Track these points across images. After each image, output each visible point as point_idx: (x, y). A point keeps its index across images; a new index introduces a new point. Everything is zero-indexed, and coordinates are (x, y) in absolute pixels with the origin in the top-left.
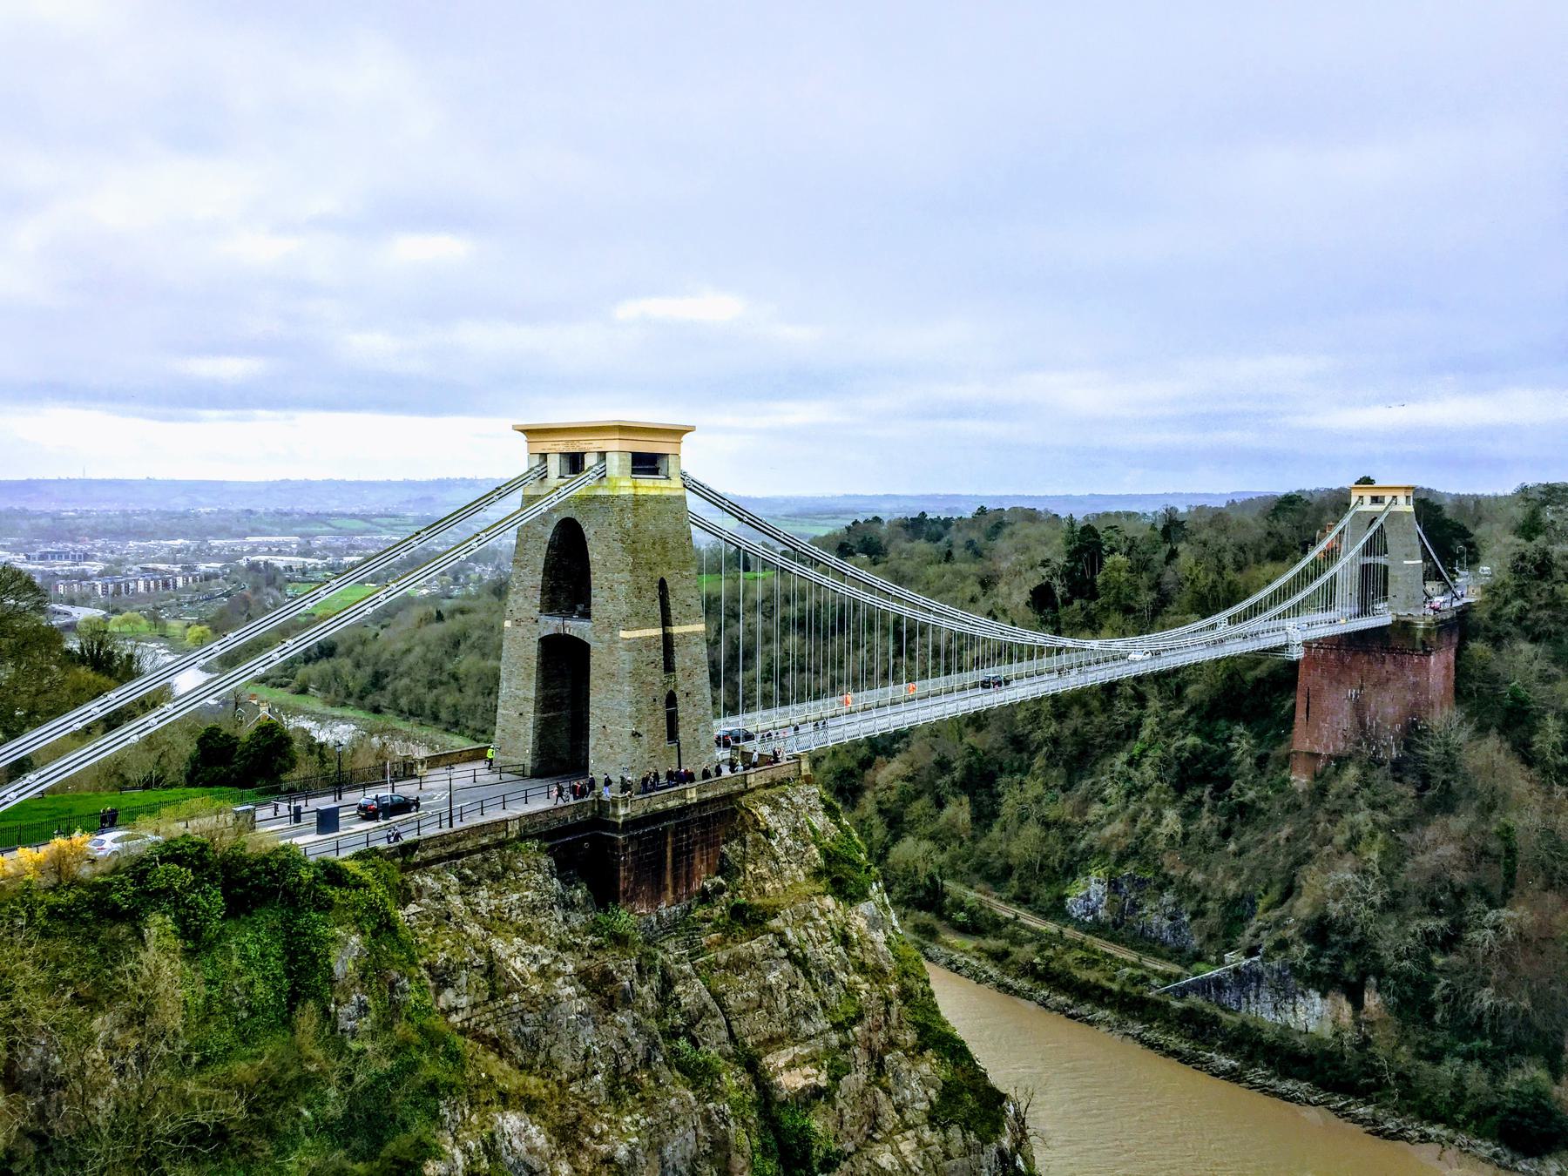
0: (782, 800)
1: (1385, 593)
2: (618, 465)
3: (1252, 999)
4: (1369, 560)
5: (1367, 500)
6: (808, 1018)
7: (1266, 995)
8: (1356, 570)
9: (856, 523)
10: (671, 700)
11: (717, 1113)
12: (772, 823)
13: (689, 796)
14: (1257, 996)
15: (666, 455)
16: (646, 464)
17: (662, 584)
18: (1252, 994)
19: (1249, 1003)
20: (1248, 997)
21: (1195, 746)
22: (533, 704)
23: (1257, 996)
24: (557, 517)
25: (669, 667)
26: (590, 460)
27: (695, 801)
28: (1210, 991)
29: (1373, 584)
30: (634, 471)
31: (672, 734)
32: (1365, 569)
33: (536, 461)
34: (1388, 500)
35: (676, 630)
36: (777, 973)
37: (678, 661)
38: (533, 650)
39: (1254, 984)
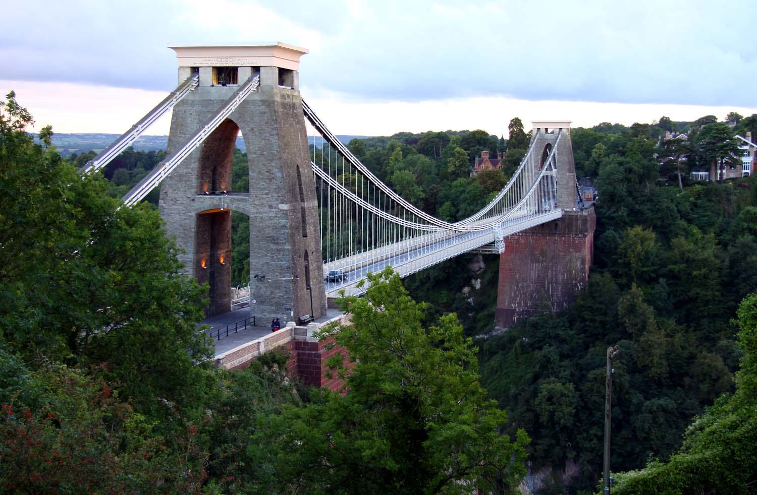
2: (270, 78)
15: (291, 71)
16: (284, 75)
29: (545, 191)
33: (189, 71)
35: (306, 205)
38: (192, 223)
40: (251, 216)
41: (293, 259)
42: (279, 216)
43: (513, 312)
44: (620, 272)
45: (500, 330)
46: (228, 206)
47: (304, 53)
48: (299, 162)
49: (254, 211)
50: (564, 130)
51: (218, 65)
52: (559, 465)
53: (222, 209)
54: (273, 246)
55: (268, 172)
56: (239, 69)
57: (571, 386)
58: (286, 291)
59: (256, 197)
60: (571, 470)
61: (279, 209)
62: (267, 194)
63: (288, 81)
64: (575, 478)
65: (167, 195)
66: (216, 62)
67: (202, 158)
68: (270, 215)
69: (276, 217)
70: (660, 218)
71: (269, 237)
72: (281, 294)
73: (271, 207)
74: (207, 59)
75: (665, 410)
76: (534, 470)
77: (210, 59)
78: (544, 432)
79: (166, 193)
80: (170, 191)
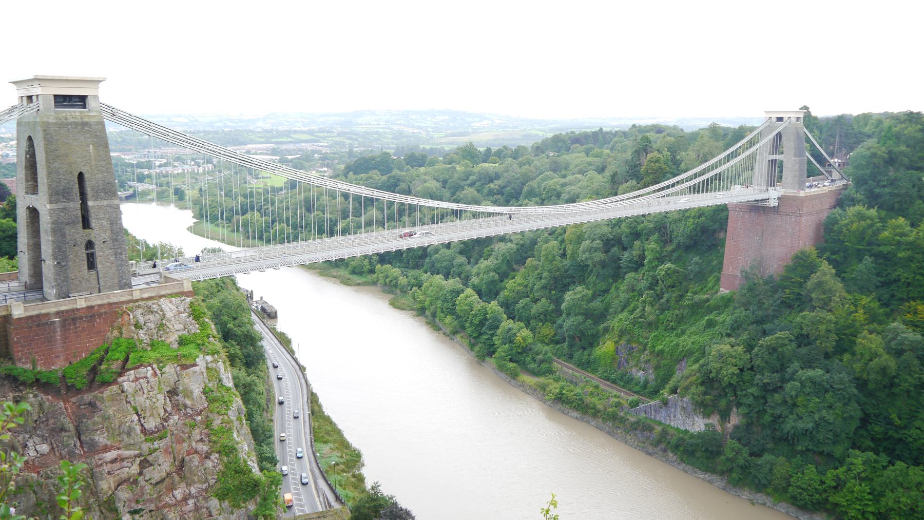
0: (154, 306)
1: (780, 178)
3: (672, 418)
4: (774, 157)
5: (774, 120)
6: (129, 434)
7: (679, 416)
8: (765, 164)
9: (567, 133)
10: (90, 245)
11: (54, 486)
12: (141, 320)
13: (78, 303)
14: (674, 416)
15: (86, 97)
17: (81, 176)
18: (672, 415)
19: (670, 420)
20: (670, 417)
21: (669, 269)
22: (26, 246)
23: (674, 416)
24: (27, 136)
25: (86, 224)
26: (34, 98)
27: (85, 306)
28: (651, 413)
29: (776, 172)
30: (56, 106)
31: (92, 265)
32: (773, 162)
33: (20, 99)
34: (785, 119)
35: (90, 203)
36: (114, 409)
37: (93, 223)
39: (673, 409)
41: (59, 248)
43: (735, 277)
44: (836, 249)
45: (724, 291)
47: (101, 81)
48: (84, 170)
50: (792, 119)
52: (725, 416)
57: (740, 349)
60: (735, 419)
63: (87, 106)
64: (736, 427)
67: (30, 165)
70: (898, 202)
75: (813, 382)
76: (707, 415)
78: (716, 385)
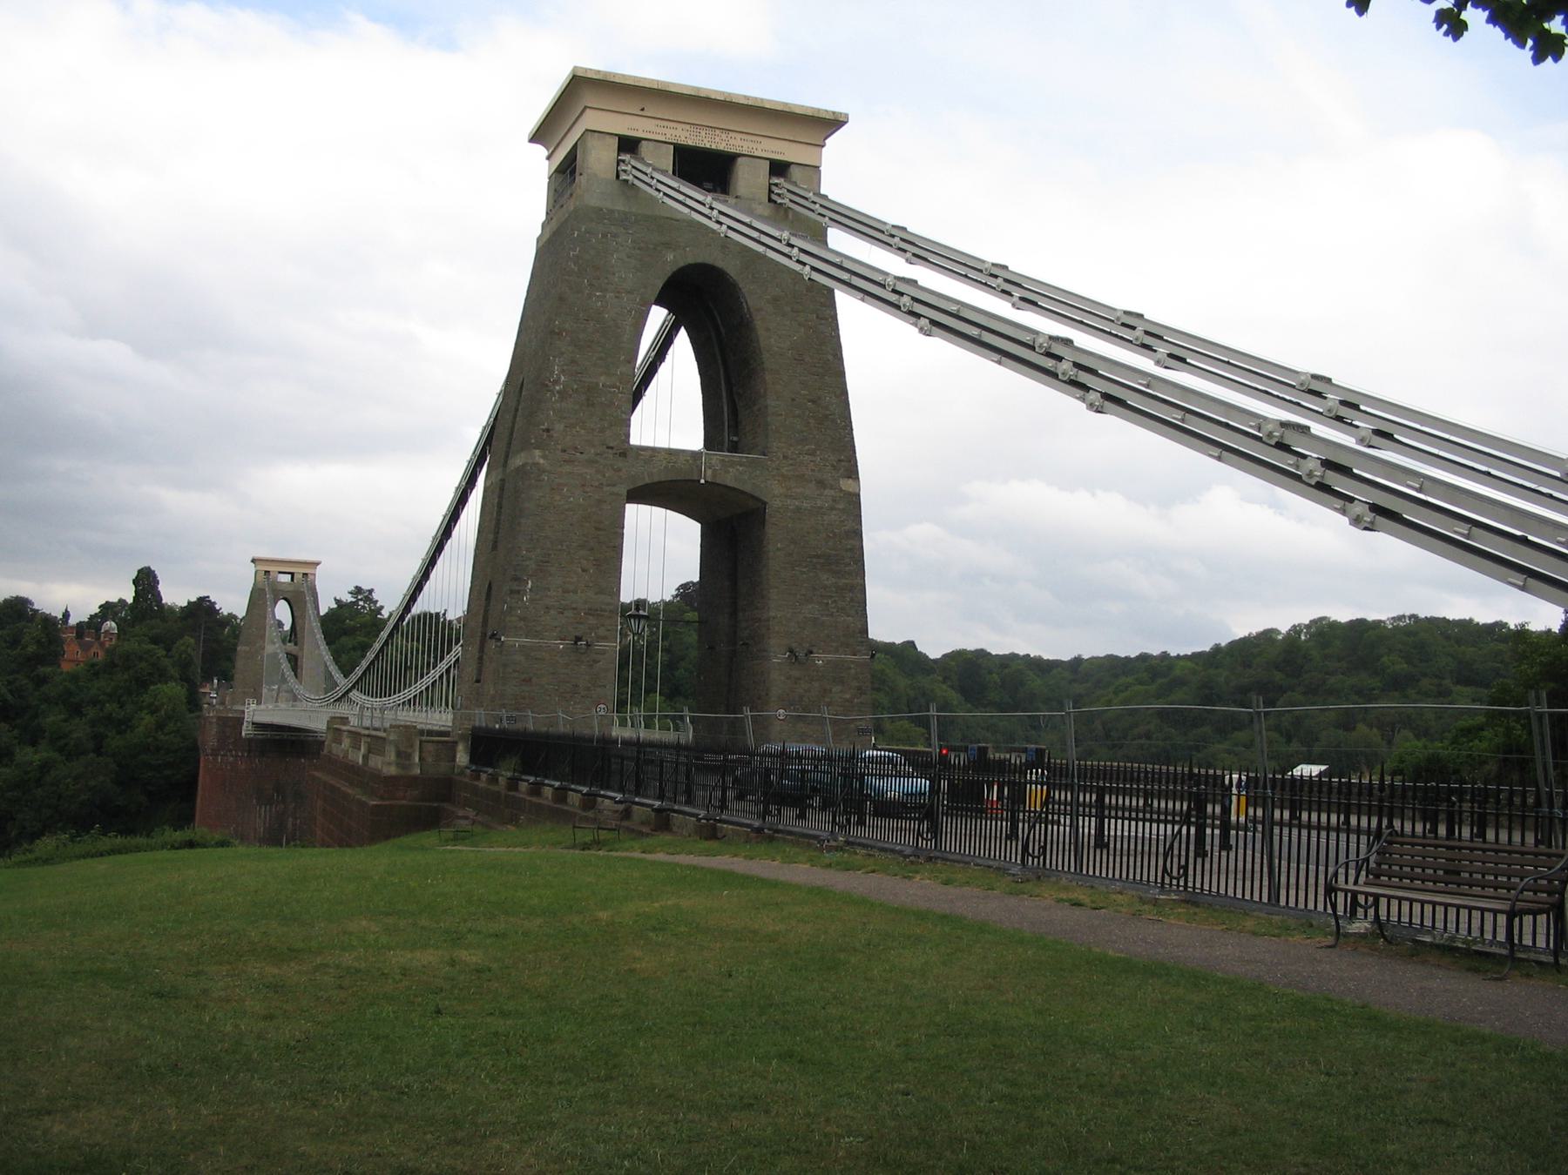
40: (774, 504)
42: (841, 506)
46: (714, 475)
49: (777, 489)
51: (690, 143)
53: (702, 481)
54: (826, 579)
55: (813, 402)
56: (740, 160)
58: (859, 688)
59: (785, 457)
61: (841, 490)
62: (812, 453)
65: (550, 437)
66: (687, 134)
68: (819, 503)
69: (832, 508)
71: (818, 557)
72: (848, 696)
73: (821, 484)
74: (666, 123)
77: (672, 124)
79: (548, 430)
80: (559, 427)
